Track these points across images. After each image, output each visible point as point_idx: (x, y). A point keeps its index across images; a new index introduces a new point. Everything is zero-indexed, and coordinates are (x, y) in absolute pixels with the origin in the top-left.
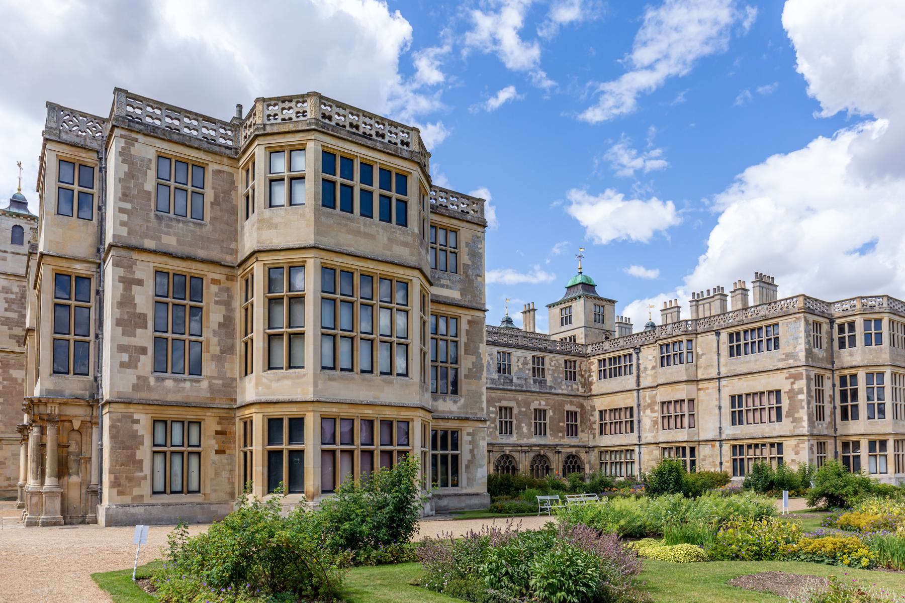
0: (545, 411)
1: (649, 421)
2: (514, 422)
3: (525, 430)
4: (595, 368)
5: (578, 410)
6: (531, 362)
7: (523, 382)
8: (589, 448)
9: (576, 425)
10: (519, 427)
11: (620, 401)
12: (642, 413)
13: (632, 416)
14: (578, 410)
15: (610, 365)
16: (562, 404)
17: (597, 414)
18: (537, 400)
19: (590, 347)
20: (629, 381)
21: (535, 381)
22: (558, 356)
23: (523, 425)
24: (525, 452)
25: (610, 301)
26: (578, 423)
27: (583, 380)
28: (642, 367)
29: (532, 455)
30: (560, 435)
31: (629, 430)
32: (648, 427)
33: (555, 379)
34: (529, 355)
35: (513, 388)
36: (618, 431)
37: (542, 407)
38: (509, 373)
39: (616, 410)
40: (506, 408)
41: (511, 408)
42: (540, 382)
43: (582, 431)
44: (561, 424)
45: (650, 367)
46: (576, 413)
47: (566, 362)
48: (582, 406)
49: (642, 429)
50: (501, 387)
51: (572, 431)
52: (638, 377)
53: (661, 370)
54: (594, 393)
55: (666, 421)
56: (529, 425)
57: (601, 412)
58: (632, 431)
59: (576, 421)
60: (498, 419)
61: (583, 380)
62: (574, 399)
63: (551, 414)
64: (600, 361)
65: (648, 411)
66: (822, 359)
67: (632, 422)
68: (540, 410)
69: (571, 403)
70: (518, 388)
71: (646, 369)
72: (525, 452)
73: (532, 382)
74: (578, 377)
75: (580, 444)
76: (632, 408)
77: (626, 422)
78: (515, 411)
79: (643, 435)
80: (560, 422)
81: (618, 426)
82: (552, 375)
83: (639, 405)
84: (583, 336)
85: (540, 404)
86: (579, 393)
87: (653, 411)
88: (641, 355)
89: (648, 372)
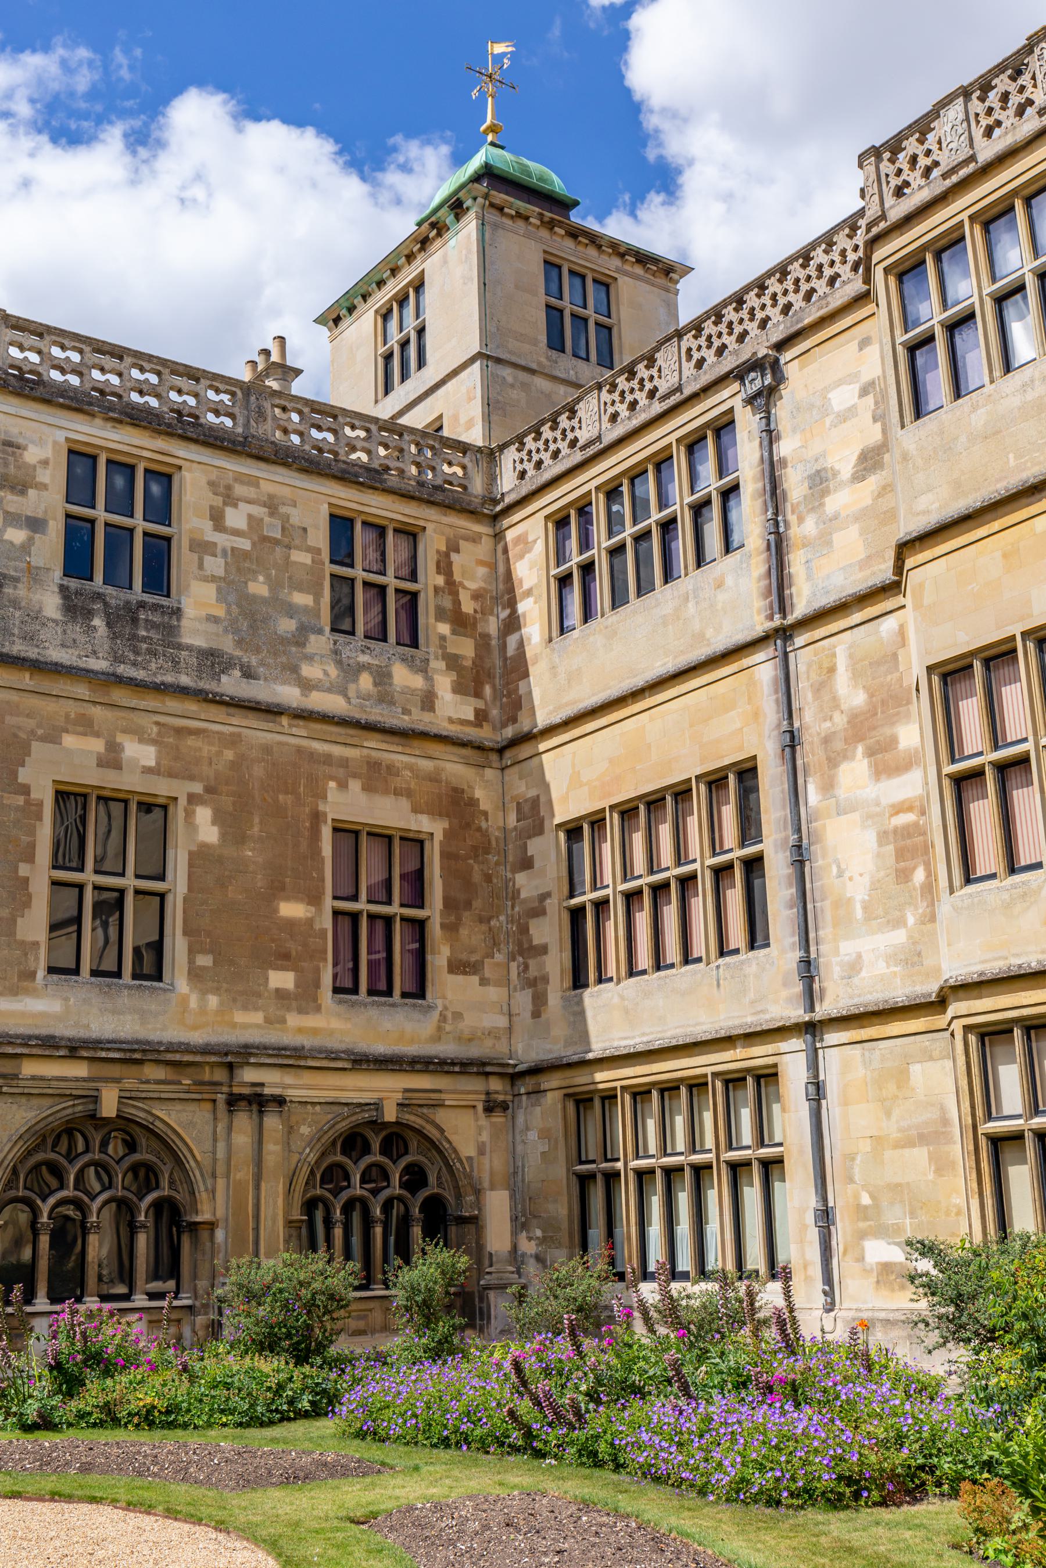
0: (158, 810)
1: (870, 838)
4: (531, 570)
5: (432, 827)
8: (514, 1077)
9: (419, 926)
11: (671, 743)
12: (813, 795)
13: (749, 826)
14: (432, 827)
15: (614, 523)
16: (303, 776)
17: (548, 850)
18: (86, 726)
19: (511, 454)
20: (724, 598)
22: (276, 480)
25: (643, 258)
27: (466, 648)
28: (795, 485)
30: (282, 979)
31: (737, 935)
32: (858, 891)
33: (248, 617)
36: (672, 951)
39: (654, 802)
42: (125, 619)
43: (457, 967)
44: (291, 910)
45: (846, 470)
47: (341, 526)
48: (457, 805)
49: (824, 909)
51: (382, 958)
52: (778, 547)
53: (913, 438)
55: (983, 813)
57: (573, 831)
58: (756, 935)
59: (418, 898)
61: (466, 648)
62: (395, 755)
63: (205, 827)
64: (561, 523)
65: (855, 773)
67: (754, 865)
69: (376, 778)
71: (820, 482)
74: (436, 628)
75: (447, 1049)
76: (747, 773)
77: (721, 872)
79: (835, 953)
80: (277, 890)
81: (670, 913)
82: (230, 587)
83: (792, 742)
84: (476, 409)
85: (112, 759)
87: (887, 762)
88: (782, 411)
89: (838, 501)
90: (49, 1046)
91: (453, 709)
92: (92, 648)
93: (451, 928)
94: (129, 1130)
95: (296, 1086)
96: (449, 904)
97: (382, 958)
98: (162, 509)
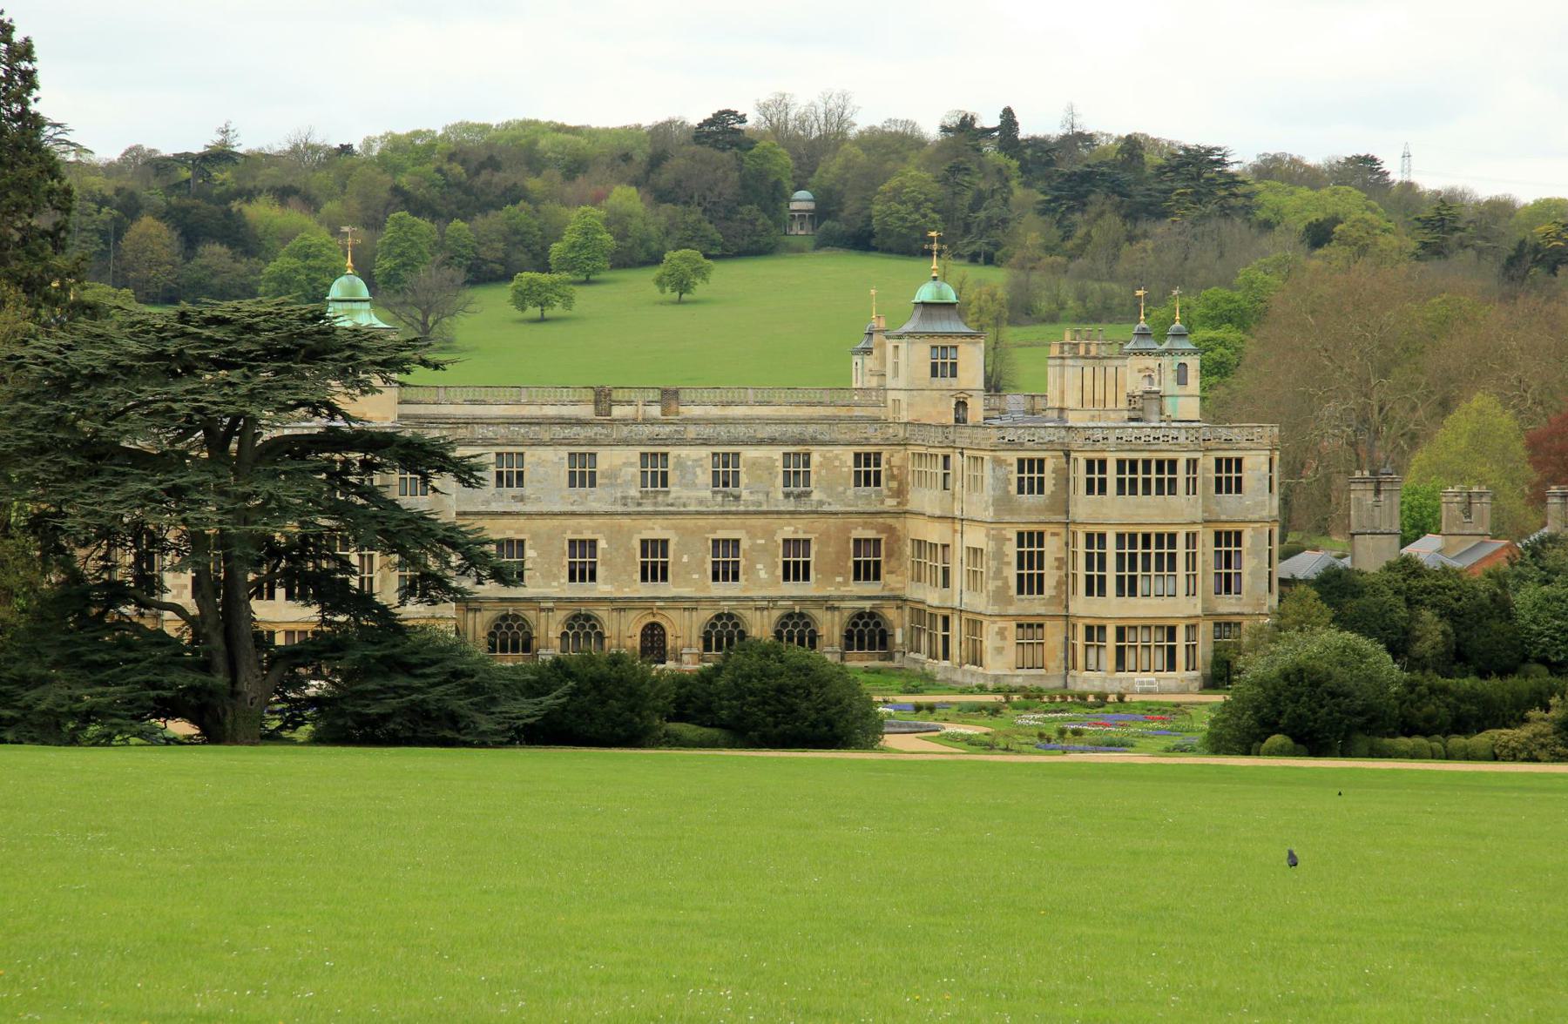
0: (807, 541)
2: (743, 563)
3: (763, 574)
5: (883, 536)
6: (780, 464)
7: (761, 497)
10: (751, 568)
21: (787, 495)
22: (837, 450)
23: (759, 566)
24: (762, 609)
26: (882, 558)
29: (776, 614)
30: (840, 579)
34: (777, 453)
35: (742, 508)
37: (801, 536)
38: (736, 484)
40: (726, 541)
41: (737, 542)
46: (878, 541)
48: (890, 530)
50: (717, 509)
51: (867, 571)
54: (908, 507)
56: (771, 569)
60: (709, 559)
66: (1039, 511)
68: (797, 541)
69: (865, 526)
70: (751, 508)
72: (762, 609)
73: (781, 496)
75: (886, 593)
78: (744, 545)
86: (884, 508)
90: (783, 598)
91: (890, 503)
92: (791, 505)
93: (887, 563)
94: (801, 615)
95: (843, 605)
96: (889, 556)
97: (867, 571)
98: (807, 464)
